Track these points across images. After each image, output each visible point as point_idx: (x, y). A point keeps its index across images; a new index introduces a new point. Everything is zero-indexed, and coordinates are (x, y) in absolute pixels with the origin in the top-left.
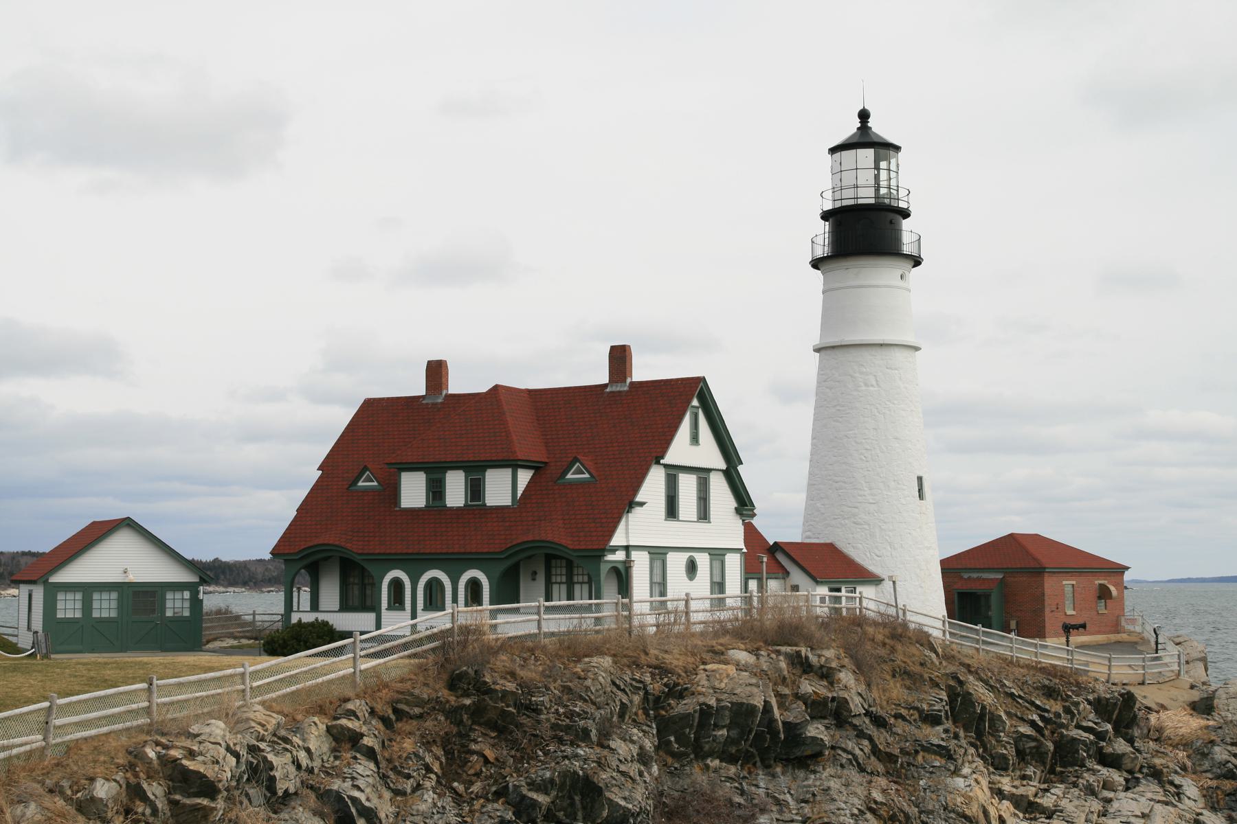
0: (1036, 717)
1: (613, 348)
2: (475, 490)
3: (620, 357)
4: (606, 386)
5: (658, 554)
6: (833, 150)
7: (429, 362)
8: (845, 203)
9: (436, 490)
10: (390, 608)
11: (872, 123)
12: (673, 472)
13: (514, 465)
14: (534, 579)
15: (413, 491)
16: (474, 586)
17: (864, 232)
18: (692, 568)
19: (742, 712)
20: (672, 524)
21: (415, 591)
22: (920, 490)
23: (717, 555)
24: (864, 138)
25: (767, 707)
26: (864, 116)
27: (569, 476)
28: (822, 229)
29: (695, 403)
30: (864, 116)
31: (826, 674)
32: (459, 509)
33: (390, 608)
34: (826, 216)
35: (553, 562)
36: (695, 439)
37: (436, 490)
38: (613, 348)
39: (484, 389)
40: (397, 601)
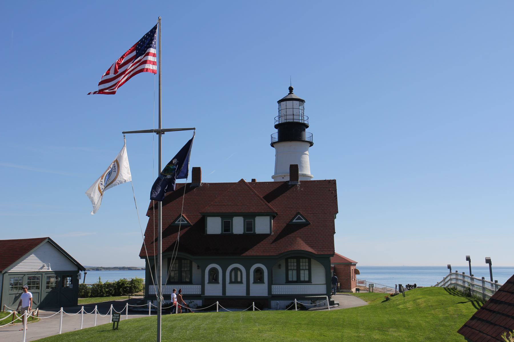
1: (292, 166)
4: (288, 182)
8: (288, 121)
9: (227, 226)
10: (210, 282)
11: (294, 91)
14: (280, 268)
15: (214, 226)
16: (259, 271)
26: (291, 89)
27: (294, 221)
28: (277, 130)
30: (291, 89)
32: (240, 235)
33: (210, 282)
34: (276, 127)
35: (289, 260)
37: (227, 226)
38: (292, 166)
39: (237, 181)
40: (214, 279)
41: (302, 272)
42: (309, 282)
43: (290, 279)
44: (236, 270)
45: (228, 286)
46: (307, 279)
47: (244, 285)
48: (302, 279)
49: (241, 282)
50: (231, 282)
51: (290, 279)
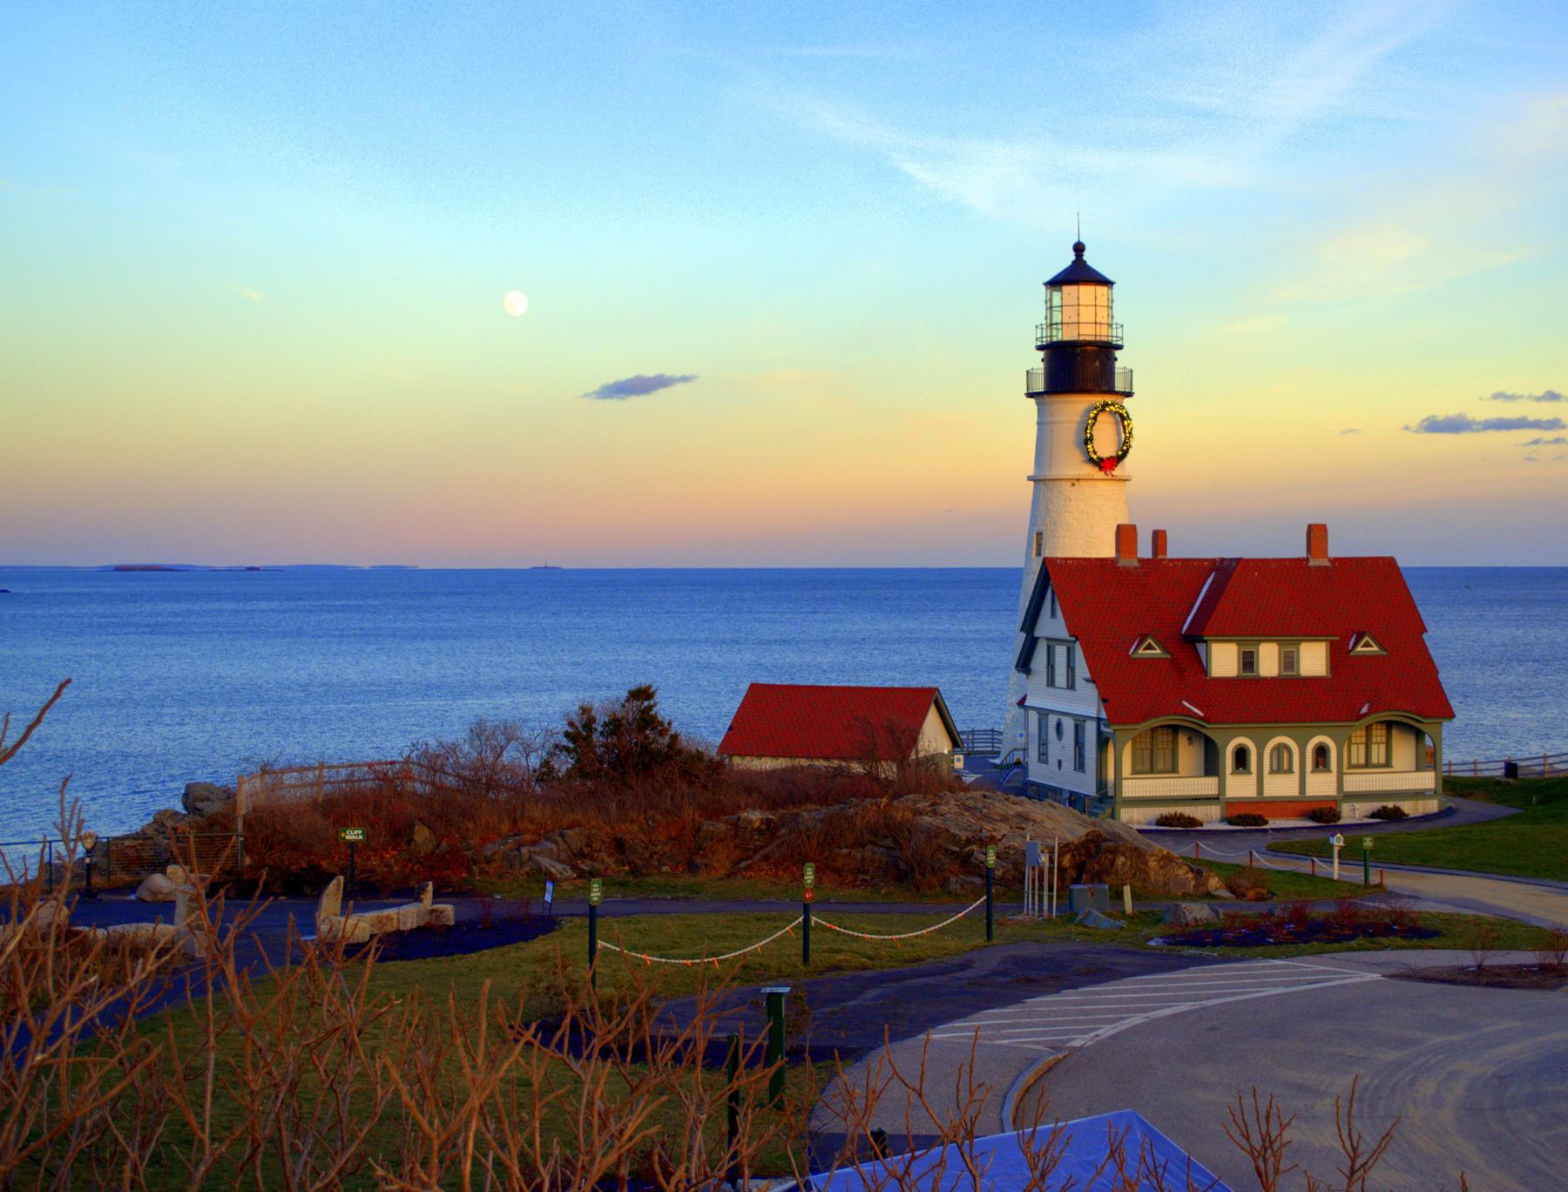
2: (1289, 661)
3: (1316, 534)
7: (1119, 527)
9: (1248, 661)
11: (1087, 257)
15: (1223, 660)
16: (1321, 752)
21: (1262, 753)
24: (1079, 273)
26: (1079, 248)
30: (1079, 248)
32: (1272, 679)
37: (1248, 661)
41: (1374, 748)
42: (1388, 764)
43: (1354, 762)
44: (1280, 748)
45: (1267, 778)
46: (1382, 761)
47: (1295, 777)
48: (1374, 760)
49: (1290, 771)
50: (1272, 772)
51: (1354, 762)
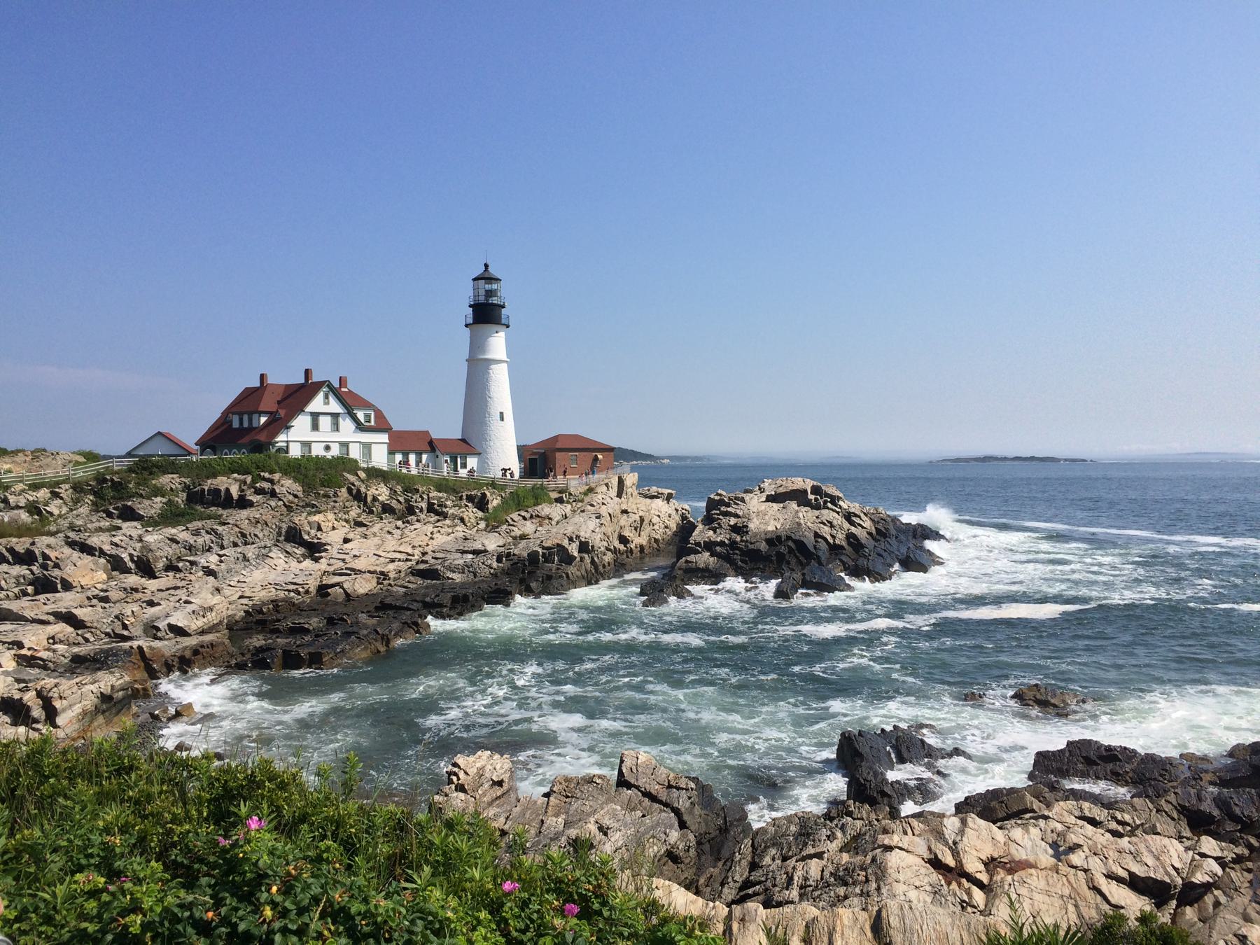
0: (401, 499)
2: (250, 420)
3: (307, 373)
5: (307, 445)
6: (474, 280)
12: (315, 416)
13: (261, 413)
17: (486, 313)
18: (327, 448)
19: (217, 491)
20: (316, 433)
22: (502, 419)
23: (345, 445)
24: (486, 277)
25: (228, 490)
26: (486, 266)
29: (325, 389)
30: (486, 266)
31: (272, 481)
36: (327, 403)
